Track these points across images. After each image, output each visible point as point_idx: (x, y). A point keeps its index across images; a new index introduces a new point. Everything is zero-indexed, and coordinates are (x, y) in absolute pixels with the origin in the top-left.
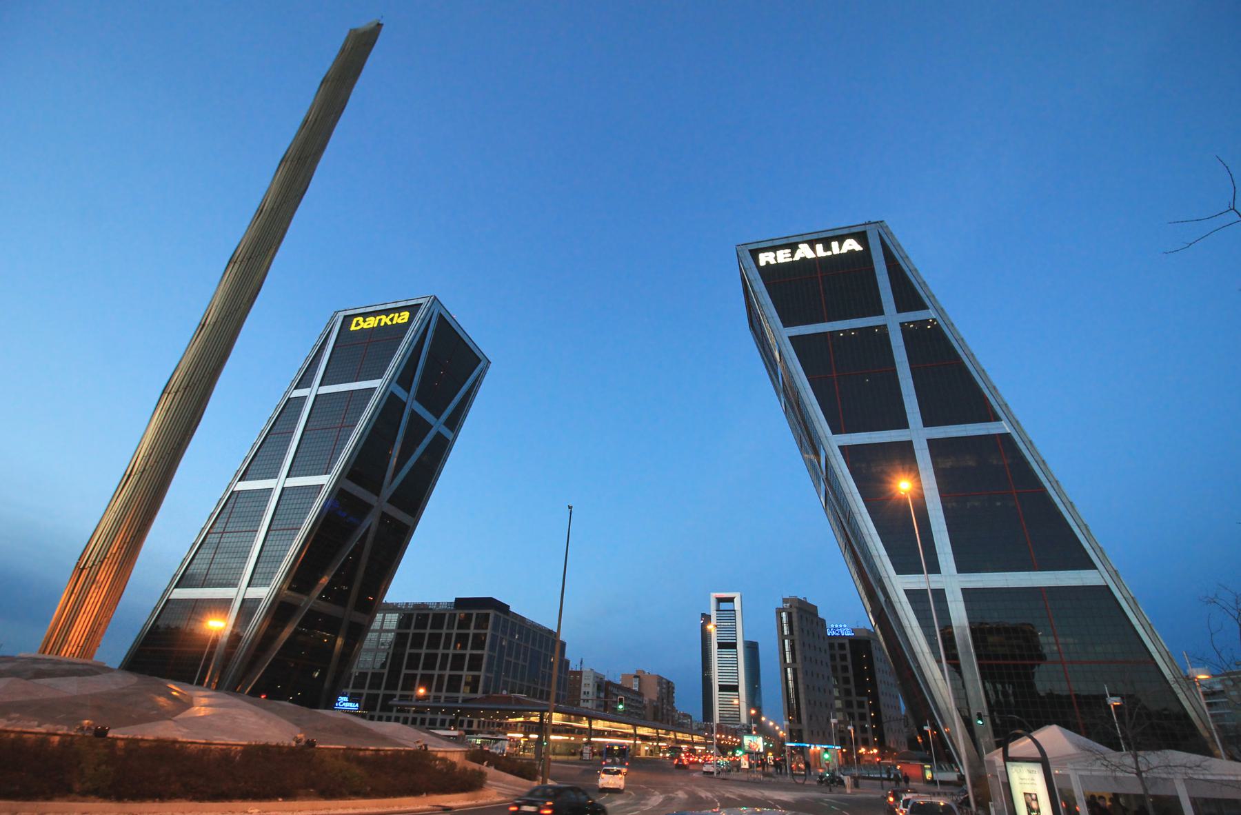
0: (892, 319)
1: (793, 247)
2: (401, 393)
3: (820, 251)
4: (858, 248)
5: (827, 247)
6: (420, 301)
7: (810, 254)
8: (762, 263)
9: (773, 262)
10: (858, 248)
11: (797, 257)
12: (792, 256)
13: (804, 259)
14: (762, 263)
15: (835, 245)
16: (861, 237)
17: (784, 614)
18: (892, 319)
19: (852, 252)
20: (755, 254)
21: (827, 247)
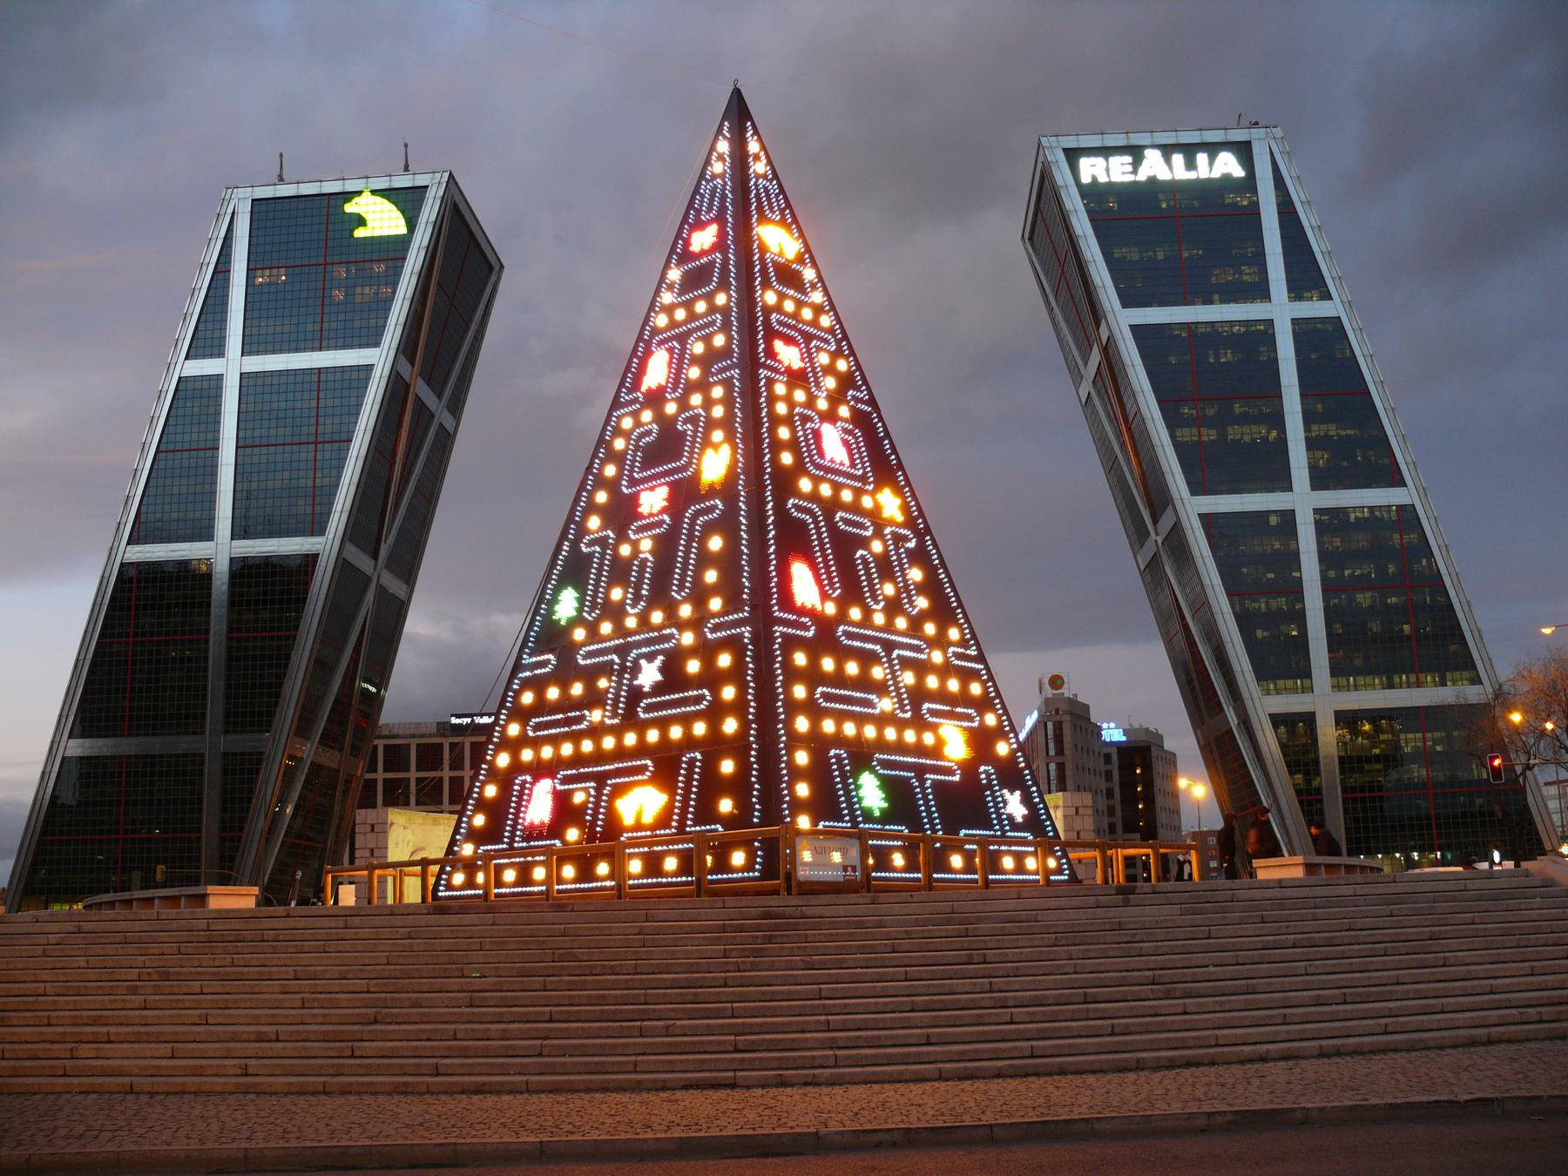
0: (1281, 310)
1: (1136, 153)
2: (405, 370)
3: (1178, 170)
4: (1238, 172)
5: (1191, 164)
6: (421, 181)
7: (1163, 174)
8: (1086, 179)
9: (1103, 179)
10: (1238, 172)
11: (1142, 176)
12: (1135, 172)
13: (1152, 180)
14: (1086, 179)
15: (1202, 158)
16: (1244, 151)
17: (1050, 725)
18: (1281, 310)
19: (1227, 178)
20: (1073, 155)
21: (1191, 164)
